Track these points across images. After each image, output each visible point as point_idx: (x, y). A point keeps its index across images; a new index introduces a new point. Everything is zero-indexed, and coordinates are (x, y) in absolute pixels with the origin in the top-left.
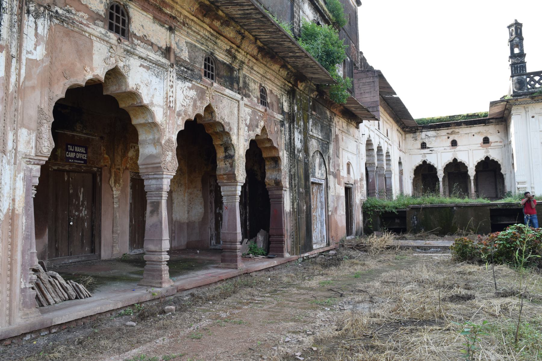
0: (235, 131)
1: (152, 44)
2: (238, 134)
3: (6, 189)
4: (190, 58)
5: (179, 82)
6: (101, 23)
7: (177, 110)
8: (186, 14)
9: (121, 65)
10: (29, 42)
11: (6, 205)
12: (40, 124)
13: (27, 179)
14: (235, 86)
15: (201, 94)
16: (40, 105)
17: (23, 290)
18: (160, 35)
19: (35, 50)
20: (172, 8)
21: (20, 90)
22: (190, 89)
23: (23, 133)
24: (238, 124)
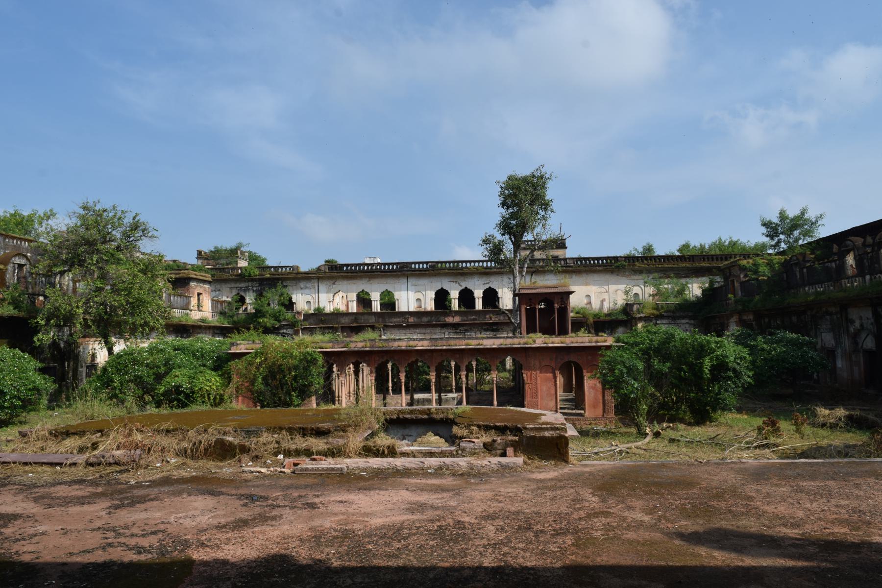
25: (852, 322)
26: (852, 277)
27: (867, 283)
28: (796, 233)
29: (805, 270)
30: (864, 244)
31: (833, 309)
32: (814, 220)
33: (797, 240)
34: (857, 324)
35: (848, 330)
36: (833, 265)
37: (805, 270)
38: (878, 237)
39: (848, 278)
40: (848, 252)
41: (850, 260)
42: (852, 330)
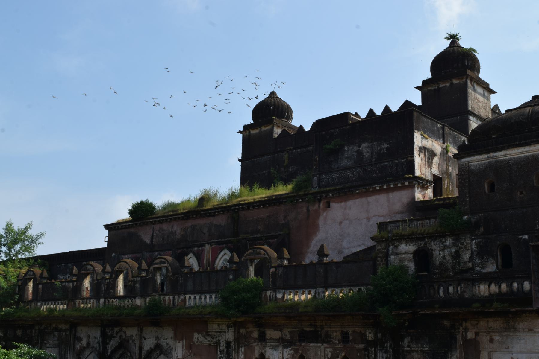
1: (273, 339)
4: (291, 337)
5: (285, 350)
8: (283, 322)
10: (240, 355)
15: (296, 351)
22: (290, 350)
25: (80, 340)
26: (87, 298)
27: (101, 306)
28: (18, 247)
29: (40, 286)
30: (104, 271)
31: (63, 327)
32: (35, 237)
33: (17, 253)
34: (84, 342)
35: (74, 348)
36: (71, 285)
37: (40, 286)
38: (117, 267)
39: (83, 299)
40: (86, 275)
41: (87, 283)
42: (78, 347)
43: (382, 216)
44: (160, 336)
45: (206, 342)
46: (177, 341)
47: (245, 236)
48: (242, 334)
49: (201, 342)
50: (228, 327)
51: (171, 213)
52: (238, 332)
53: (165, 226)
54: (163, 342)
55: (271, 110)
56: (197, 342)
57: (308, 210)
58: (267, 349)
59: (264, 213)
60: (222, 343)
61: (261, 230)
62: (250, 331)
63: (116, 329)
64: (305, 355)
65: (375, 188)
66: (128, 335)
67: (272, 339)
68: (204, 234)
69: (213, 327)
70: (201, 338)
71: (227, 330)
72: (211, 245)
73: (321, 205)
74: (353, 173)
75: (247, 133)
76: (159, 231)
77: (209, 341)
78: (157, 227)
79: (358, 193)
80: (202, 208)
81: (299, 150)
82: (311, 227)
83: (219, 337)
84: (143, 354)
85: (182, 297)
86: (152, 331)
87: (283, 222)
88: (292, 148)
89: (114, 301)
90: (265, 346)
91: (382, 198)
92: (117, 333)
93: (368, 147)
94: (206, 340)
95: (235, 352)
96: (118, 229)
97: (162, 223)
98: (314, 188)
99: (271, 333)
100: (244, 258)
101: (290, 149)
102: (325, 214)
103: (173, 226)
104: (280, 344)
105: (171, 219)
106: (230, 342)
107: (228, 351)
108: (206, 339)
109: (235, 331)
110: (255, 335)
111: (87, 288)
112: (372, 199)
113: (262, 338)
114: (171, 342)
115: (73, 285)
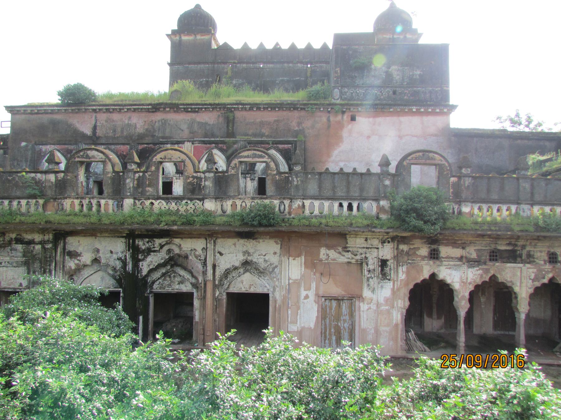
0: (518, 284)
1: (452, 258)
2: (520, 286)
3: (395, 317)
4: (478, 256)
5: (470, 270)
6: (426, 259)
7: (469, 281)
9: (436, 271)
11: (394, 322)
12: (404, 298)
13: (402, 314)
14: (519, 259)
15: (487, 271)
16: (405, 292)
17: (401, 345)
18: (457, 252)
19: (402, 276)
20: (461, 240)
21: (398, 289)
22: (477, 270)
23: (400, 301)
24: (521, 280)
43: (416, 136)
44: (251, 251)
45: (343, 259)
46: (291, 258)
47: (246, 137)
48: (402, 251)
49: (334, 260)
50: (383, 242)
51: (128, 103)
52: (397, 249)
53: (116, 116)
54: (255, 258)
55: (196, 23)
56: (327, 259)
57: (329, 120)
58: (442, 268)
59: (270, 117)
60: (370, 262)
61: (267, 134)
62: (414, 248)
63: (158, 242)
64: (498, 276)
65: (412, 109)
66: (184, 249)
67: (449, 258)
68: (182, 130)
69: (356, 242)
70: (333, 254)
71: (380, 246)
72: (193, 144)
73: (345, 117)
74: (381, 92)
75: (178, 38)
76: (106, 121)
77: (348, 258)
78: (102, 117)
79: (391, 112)
80: (180, 102)
81: (244, 65)
82: (332, 136)
83: (366, 253)
84: (218, 273)
85: (298, 203)
86: (235, 244)
87: (297, 128)
88: (236, 61)
89: (156, 203)
90: (441, 265)
91: (416, 120)
92: (162, 246)
93: (398, 70)
94: (342, 257)
95: (394, 273)
96: (32, 113)
97: (111, 112)
98: (334, 99)
99: (444, 251)
100: (408, 161)
101: (234, 63)
102: (350, 126)
103: (130, 118)
104: (464, 264)
105: (128, 109)
106: (387, 260)
107: (382, 270)
108: (344, 256)
109: (394, 248)
110: (424, 251)
111: (82, 182)
112: (405, 120)
113: (434, 255)
114: (274, 260)
115: (56, 177)
